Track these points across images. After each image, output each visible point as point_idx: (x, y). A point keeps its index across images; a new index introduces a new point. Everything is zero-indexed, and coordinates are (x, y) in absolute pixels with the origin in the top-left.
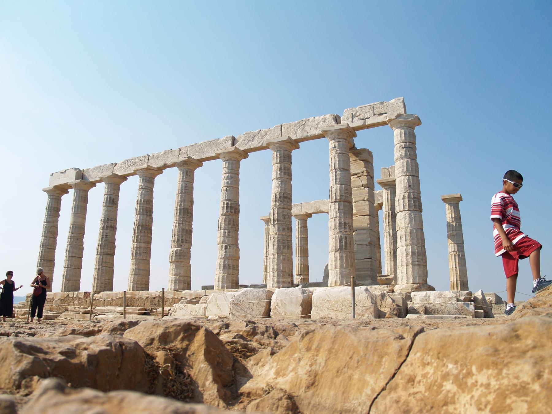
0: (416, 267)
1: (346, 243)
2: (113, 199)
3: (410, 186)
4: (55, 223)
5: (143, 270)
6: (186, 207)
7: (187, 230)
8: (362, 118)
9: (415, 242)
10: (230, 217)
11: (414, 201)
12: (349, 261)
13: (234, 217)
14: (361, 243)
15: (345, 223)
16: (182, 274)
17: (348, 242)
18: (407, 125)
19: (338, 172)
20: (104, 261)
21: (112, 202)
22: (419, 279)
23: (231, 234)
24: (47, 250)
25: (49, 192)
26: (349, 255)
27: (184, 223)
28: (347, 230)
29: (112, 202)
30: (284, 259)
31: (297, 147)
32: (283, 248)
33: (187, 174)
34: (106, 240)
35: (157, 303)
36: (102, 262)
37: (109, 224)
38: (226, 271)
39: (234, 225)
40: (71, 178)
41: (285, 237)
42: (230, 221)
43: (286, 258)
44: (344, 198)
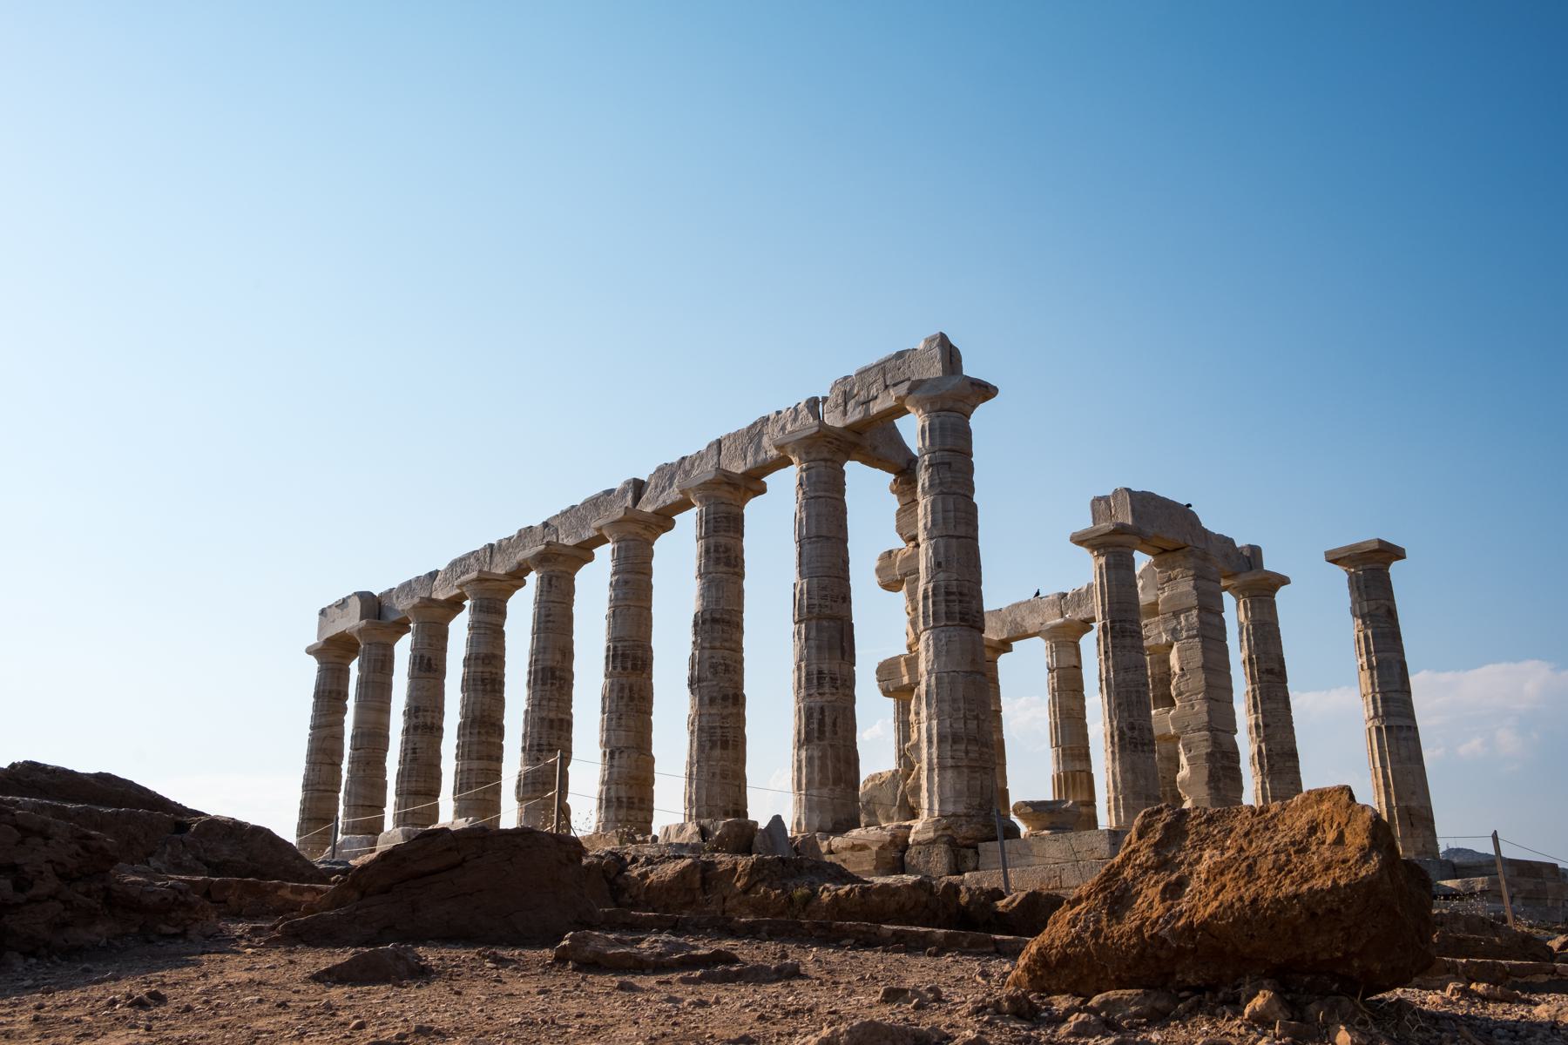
0: (949, 774)
1: (821, 723)
3: (938, 564)
4: (335, 729)
6: (549, 663)
7: (551, 721)
9: (946, 707)
10: (624, 680)
13: (633, 679)
15: (820, 672)
17: (828, 721)
18: (938, 406)
19: (806, 547)
21: (429, 667)
22: (955, 803)
23: (623, 722)
24: (316, 794)
26: (829, 752)
28: (826, 689)
29: (429, 667)
31: (762, 490)
34: (414, 760)
37: (421, 720)
38: (612, 815)
39: (631, 699)
40: (352, 621)
42: (622, 689)
44: (816, 610)
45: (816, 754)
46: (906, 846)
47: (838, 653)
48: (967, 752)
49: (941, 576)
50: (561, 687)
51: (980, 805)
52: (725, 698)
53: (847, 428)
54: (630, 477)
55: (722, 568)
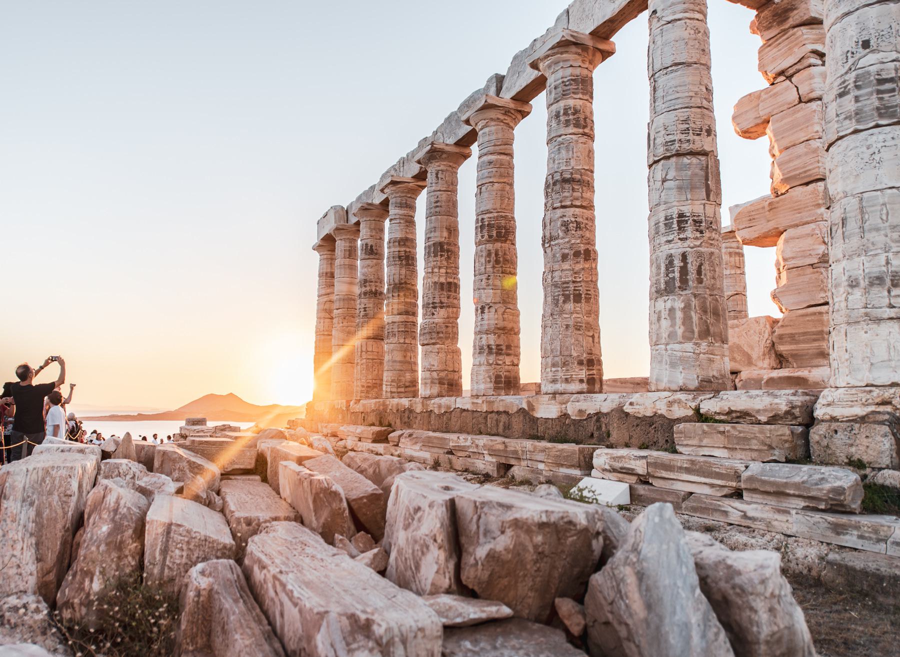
1: (684, 271)
2: (371, 246)
5: (400, 362)
6: (437, 240)
7: (442, 284)
10: (490, 246)
11: (879, 92)
13: (498, 245)
14: (799, 263)
15: (681, 215)
17: (692, 268)
20: (364, 349)
23: (490, 282)
25: (318, 248)
26: (694, 302)
27: (436, 270)
28: (690, 232)
30: (567, 326)
32: (564, 302)
33: (437, 177)
35: (406, 420)
36: (362, 352)
37: (368, 289)
39: (497, 262)
41: (570, 273)
43: (571, 323)
45: (679, 305)
46: (810, 421)
47: (703, 194)
49: (872, 58)
50: (449, 258)
52: (577, 254)
54: (492, 74)
55: (571, 129)
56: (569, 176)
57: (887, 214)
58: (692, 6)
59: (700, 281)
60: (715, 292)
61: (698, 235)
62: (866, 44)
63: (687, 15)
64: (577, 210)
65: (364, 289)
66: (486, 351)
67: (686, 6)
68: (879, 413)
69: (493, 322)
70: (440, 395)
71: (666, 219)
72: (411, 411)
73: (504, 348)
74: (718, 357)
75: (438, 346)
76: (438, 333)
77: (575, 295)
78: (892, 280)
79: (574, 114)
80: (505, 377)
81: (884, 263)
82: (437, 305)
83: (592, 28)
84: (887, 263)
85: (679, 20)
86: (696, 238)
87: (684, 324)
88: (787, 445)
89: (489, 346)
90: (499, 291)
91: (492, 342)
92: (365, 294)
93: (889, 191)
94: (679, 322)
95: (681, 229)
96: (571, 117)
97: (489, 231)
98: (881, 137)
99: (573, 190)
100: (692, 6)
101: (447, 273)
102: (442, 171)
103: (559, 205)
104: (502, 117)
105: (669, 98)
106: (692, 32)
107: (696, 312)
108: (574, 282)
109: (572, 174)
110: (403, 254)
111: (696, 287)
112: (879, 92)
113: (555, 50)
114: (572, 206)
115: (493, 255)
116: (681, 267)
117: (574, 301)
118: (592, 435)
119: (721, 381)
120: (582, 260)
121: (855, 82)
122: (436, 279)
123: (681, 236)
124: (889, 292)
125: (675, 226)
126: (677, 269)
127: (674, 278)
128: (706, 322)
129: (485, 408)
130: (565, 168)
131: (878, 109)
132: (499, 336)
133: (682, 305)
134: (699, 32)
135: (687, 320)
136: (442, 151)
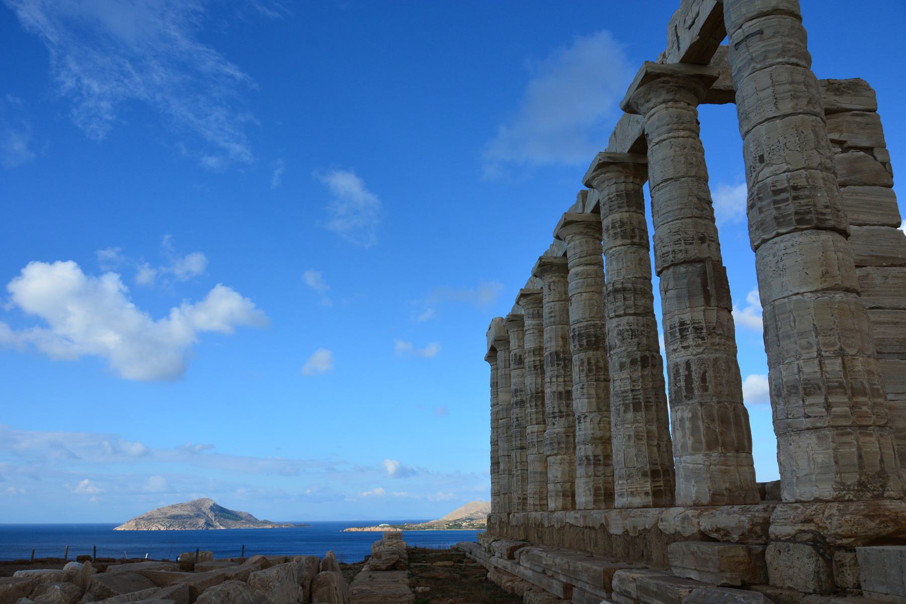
1: (689, 379)
2: (520, 356)
6: (553, 349)
7: (560, 393)
8: (689, 23)
11: (775, 202)
12: (702, 428)
15: (682, 324)
16: (559, 479)
17: (695, 376)
23: (585, 391)
27: (554, 379)
30: (629, 436)
32: (625, 412)
33: (550, 289)
37: (519, 398)
39: (590, 370)
43: (632, 433)
47: (701, 300)
48: (828, 407)
49: (767, 171)
51: (861, 484)
52: (633, 362)
53: (684, 61)
55: (619, 242)
56: (620, 286)
57: (795, 321)
58: (675, 126)
59: (705, 389)
60: (723, 399)
61: (701, 342)
62: (761, 159)
63: (671, 135)
64: (631, 317)
65: (515, 399)
66: (585, 463)
67: (669, 127)
68: (804, 531)
69: (590, 432)
70: (564, 509)
71: (671, 328)
72: (541, 525)
73: (602, 458)
74: (732, 468)
75: (560, 457)
76: (559, 443)
77: (634, 404)
78: (804, 389)
79: (621, 227)
80: (605, 489)
81: (796, 371)
82: (557, 414)
83: (629, 147)
84: (799, 371)
85: (665, 140)
86: (698, 346)
87: (692, 434)
88: (742, 567)
89: (587, 457)
90: (594, 400)
91: (590, 453)
92: (517, 403)
93: (794, 298)
94: (688, 433)
95: (683, 337)
96: (619, 230)
97: (580, 341)
98: (782, 245)
99: (625, 299)
100: (675, 126)
101: (565, 381)
102: (554, 282)
103: (612, 315)
104: (585, 231)
105: (663, 212)
106: (678, 149)
107: (703, 422)
108: (632, 390)
109: (622, 283)
110: (538, 363)
111: (701, 396)
112: (775, 202)
113: (599, 171)
114: (626, 314)
115: (586, 364)
116: (686, 376)
117: (634, 411)
118: (643, 555)
119: (736, 494)
120: (640, 368)
121: (758, 194)
122: (554, 389)
123: (684, 344)
124: (803, 401)
125: (678, 334)
126: (682, 378)
127: (680, 387)
128: (715, 431)
129: (581, 523)
130: (615, 278)
131: (776, 218)
132: (596, 446)
133: (690, 415)
134: (685, 148)
135: (695, 430)
136: (551, 264)
